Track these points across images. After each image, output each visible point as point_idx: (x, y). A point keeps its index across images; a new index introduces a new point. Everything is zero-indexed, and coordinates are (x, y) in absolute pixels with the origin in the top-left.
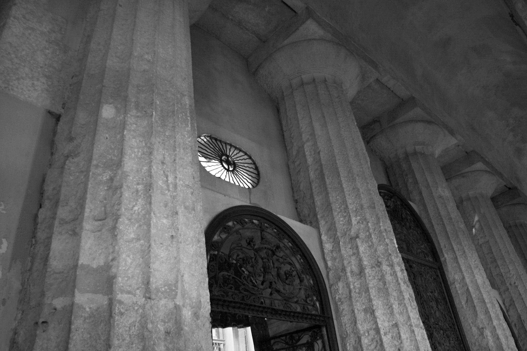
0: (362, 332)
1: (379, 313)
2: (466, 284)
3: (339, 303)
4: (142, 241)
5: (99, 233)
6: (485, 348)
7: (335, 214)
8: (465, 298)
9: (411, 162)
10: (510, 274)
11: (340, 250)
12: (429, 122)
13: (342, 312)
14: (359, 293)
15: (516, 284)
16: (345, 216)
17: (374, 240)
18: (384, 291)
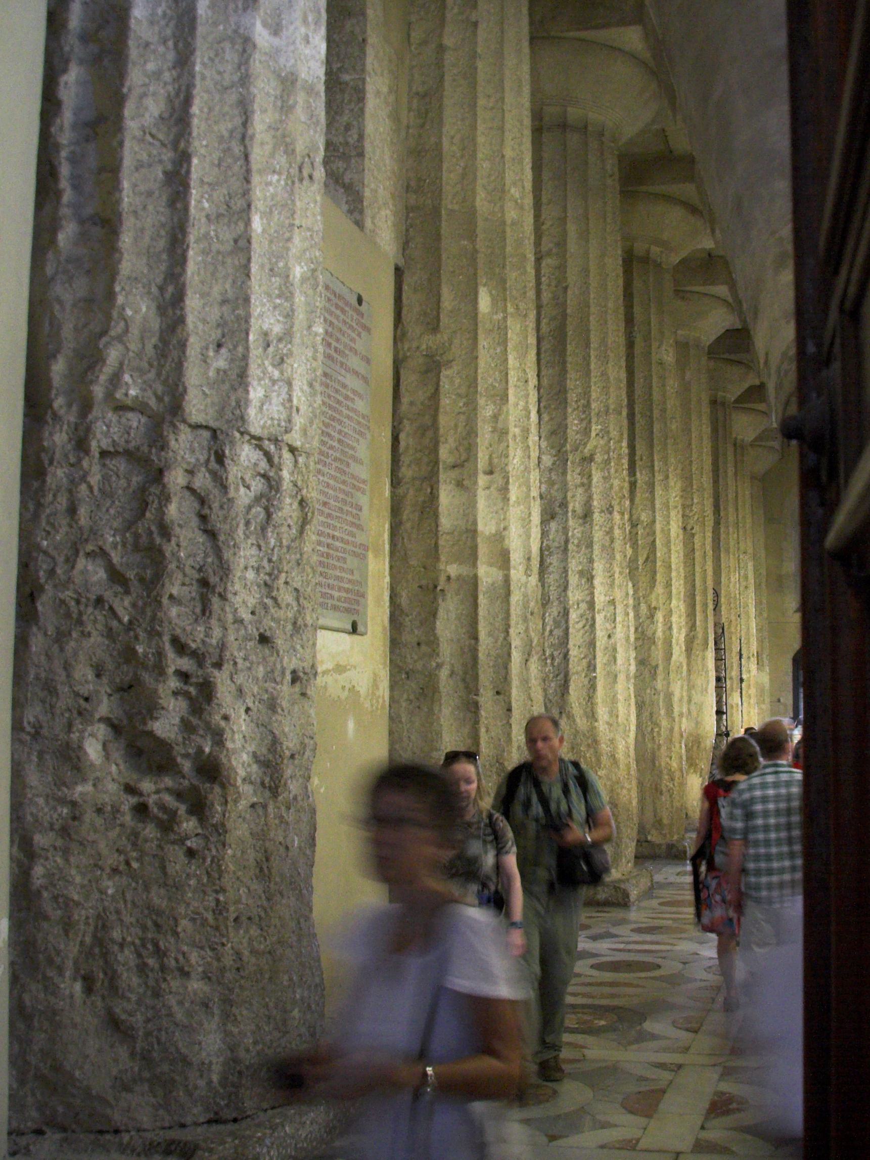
0: (571, 602)
1: (597, 582)
2: (654, 533)
3: (546, 553)
4: (522, 507)
5: (488, 492)
6: (649, 638)
7: (569, 410)
8: (645, 556)
9: (635, 274)
10: (691, 511)
11: (564, 473)
12: (694, 210)
13: (548, 567)
14: (578, 546)
15: (693, 531)
16: (582, 420)
17: (612, 471)
18: (609, 550)
